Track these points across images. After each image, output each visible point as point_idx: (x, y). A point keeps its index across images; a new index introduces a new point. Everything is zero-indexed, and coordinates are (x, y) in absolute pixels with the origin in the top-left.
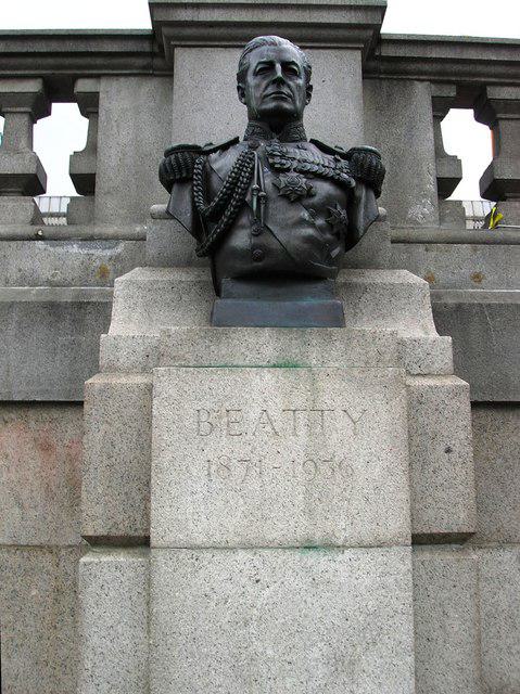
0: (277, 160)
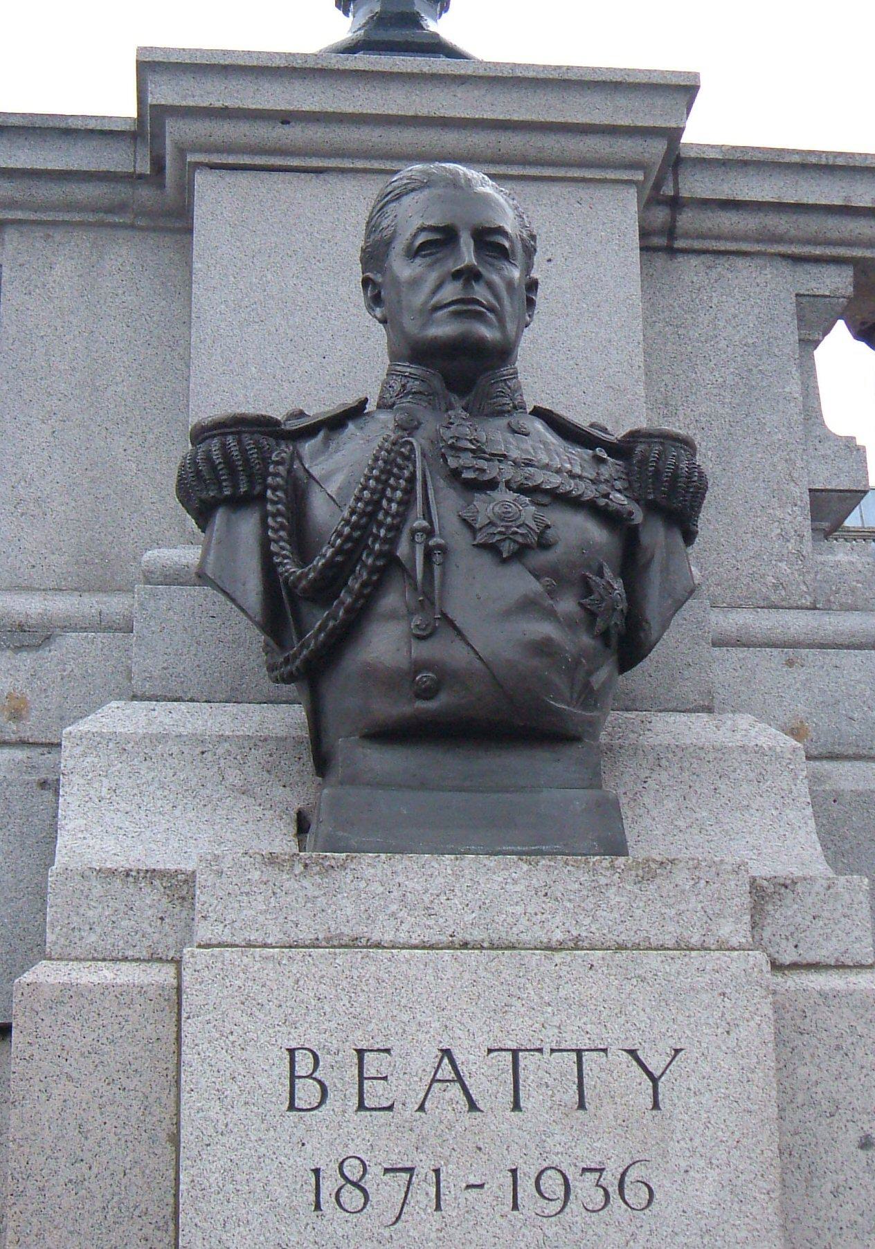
0: (466, 460)
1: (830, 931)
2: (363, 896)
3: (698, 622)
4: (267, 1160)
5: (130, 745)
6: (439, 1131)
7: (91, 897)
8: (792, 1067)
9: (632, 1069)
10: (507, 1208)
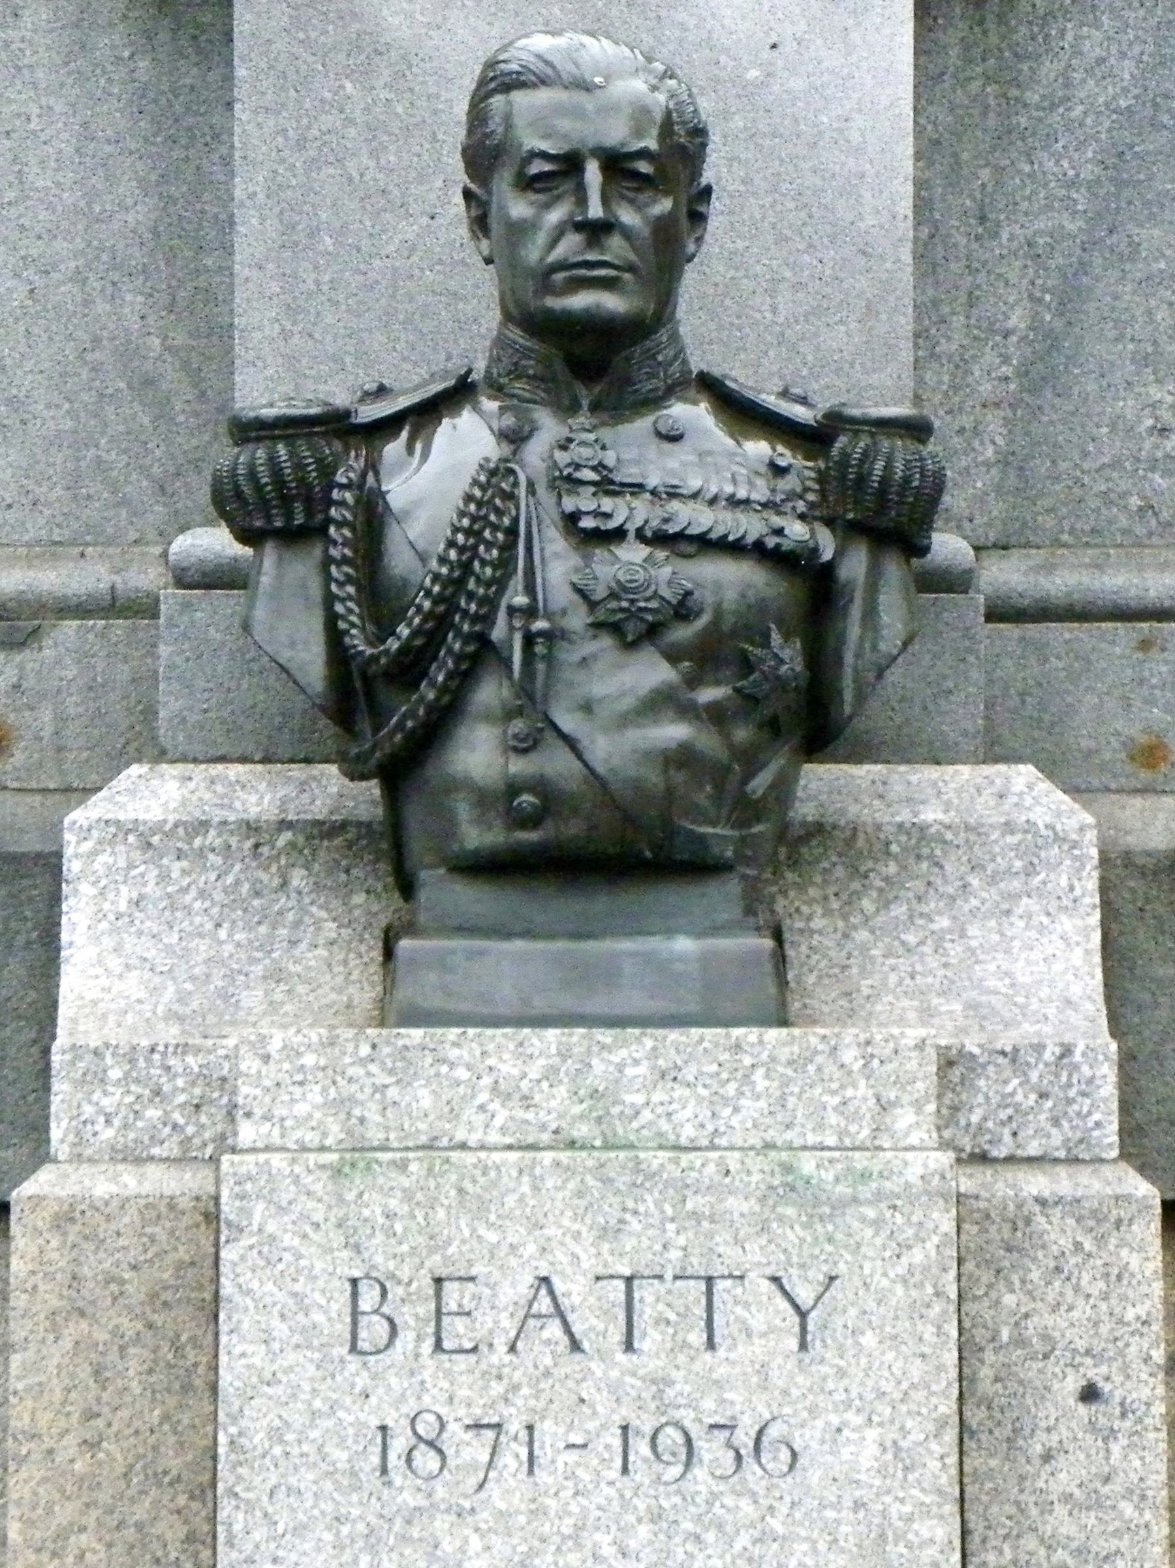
0: (585, 501)
10: (614, 1473)
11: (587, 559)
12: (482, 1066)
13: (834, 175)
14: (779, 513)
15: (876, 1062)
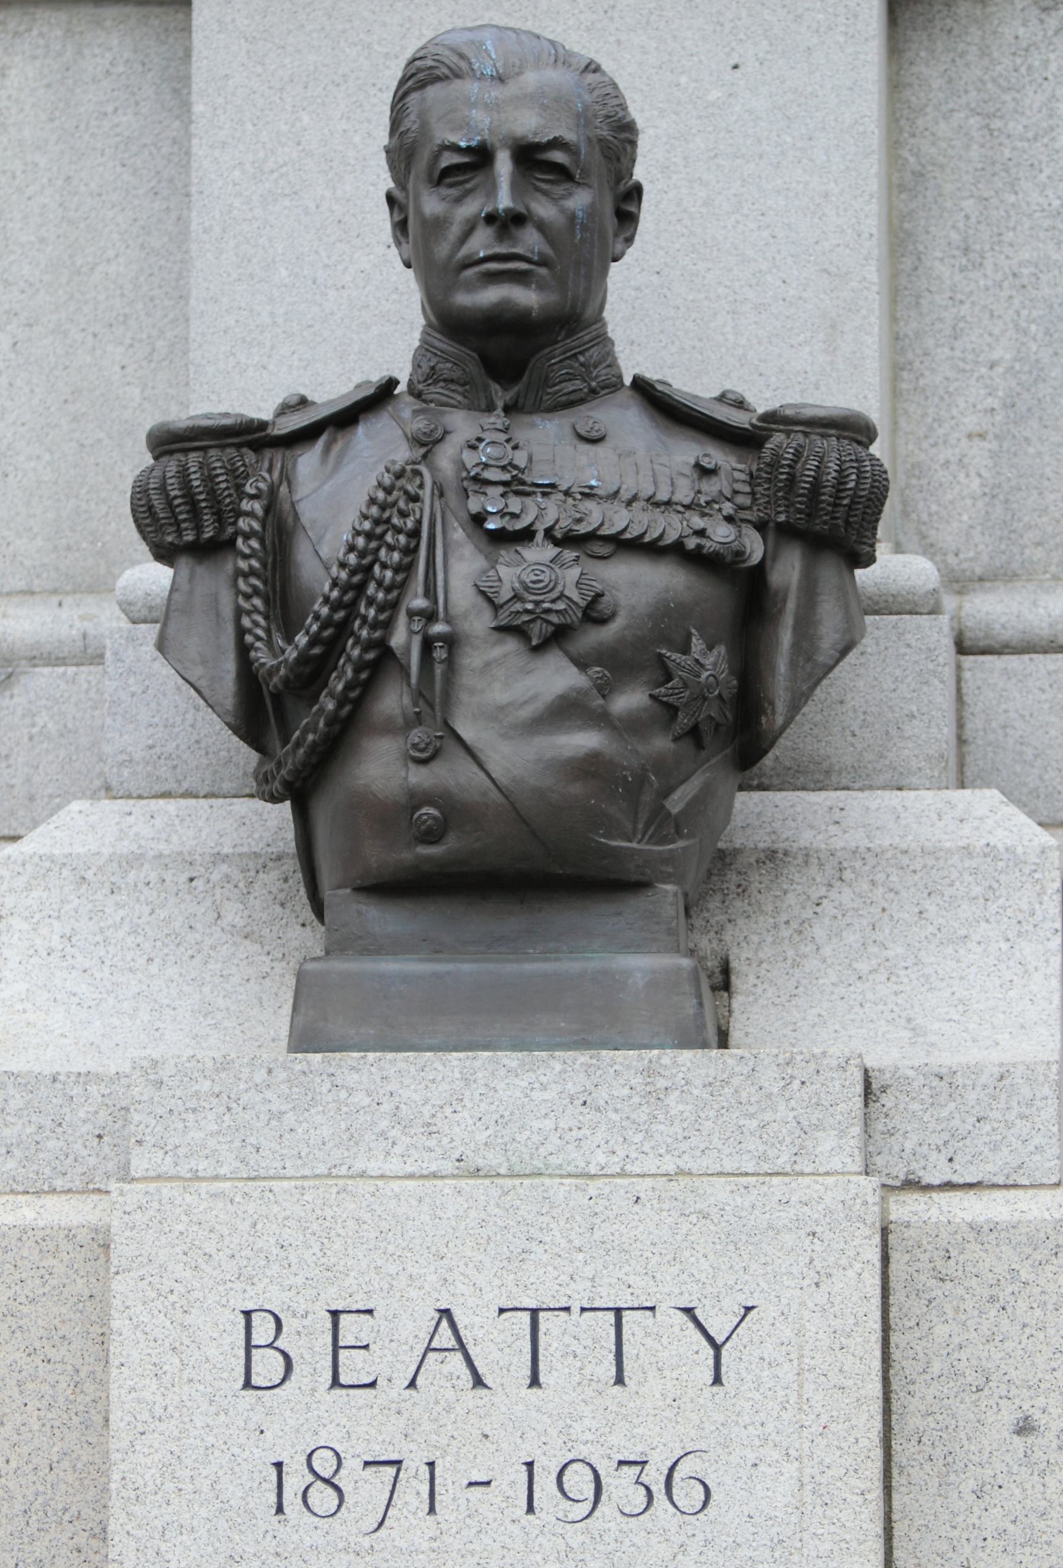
1: (999, 1137)
2: (345, 1109)
3: (929, 650)
4: (217, 1453)
5: (91, 872)
6: (435, 1414)
7: (8, 1110)
8: (928, 1324)
9: (686, 1333)
11: (493, 564)
12: (382, 1092)
13: (797, 194)
14: (703, 515)
15: (796, 1084)
